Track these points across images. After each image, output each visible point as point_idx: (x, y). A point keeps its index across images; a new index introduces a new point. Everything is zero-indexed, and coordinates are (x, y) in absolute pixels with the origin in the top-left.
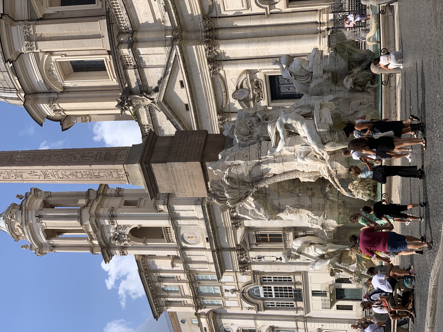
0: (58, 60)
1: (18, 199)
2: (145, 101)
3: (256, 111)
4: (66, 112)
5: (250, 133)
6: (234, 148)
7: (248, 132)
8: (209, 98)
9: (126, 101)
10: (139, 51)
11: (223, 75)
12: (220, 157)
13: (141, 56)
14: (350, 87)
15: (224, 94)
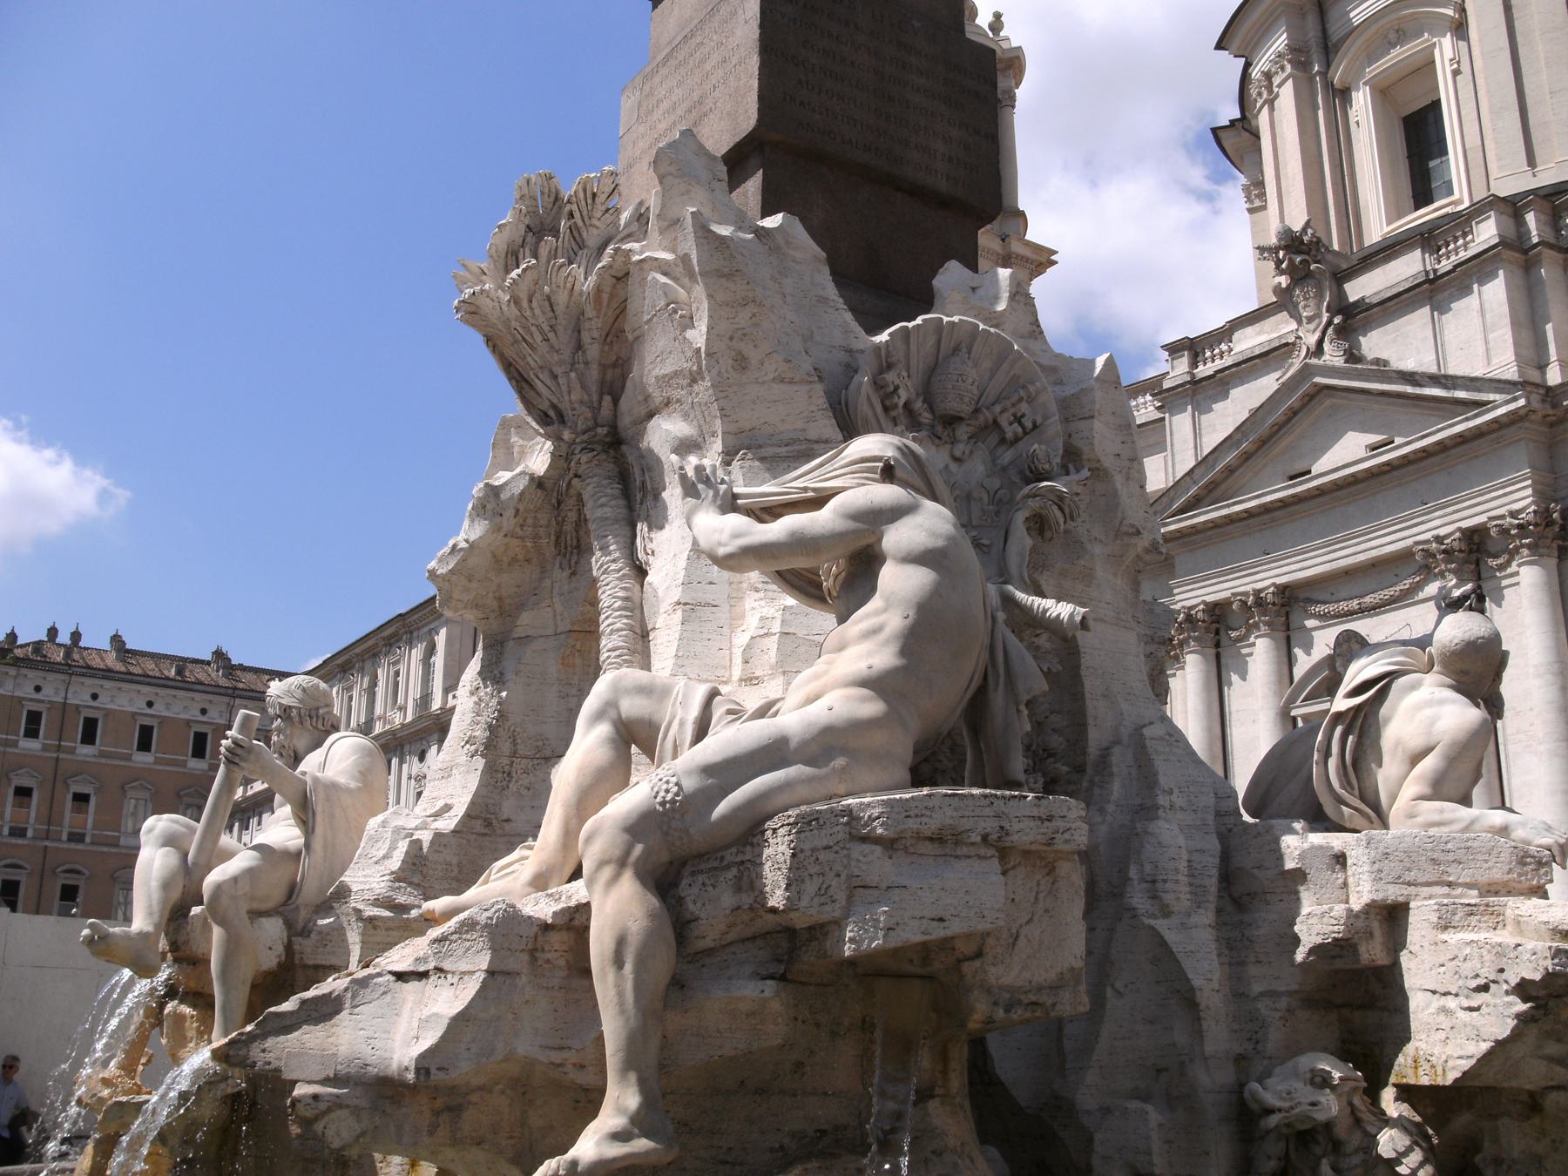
0: (1437, 52)
1: (990, 18)
2: (1312, 326)
3: (1118, 480)
4: (1265, 110)
5: (951, 421)
6: (840, 319)
7: (952, 405)
8: (1335, 551)
9: (1307, 257)
10: (1492, 276)
11: (1421, 595)
12: (773, 221)
13: (1475, 286)
14: (1270, 1099)
15: (1354, 604)
